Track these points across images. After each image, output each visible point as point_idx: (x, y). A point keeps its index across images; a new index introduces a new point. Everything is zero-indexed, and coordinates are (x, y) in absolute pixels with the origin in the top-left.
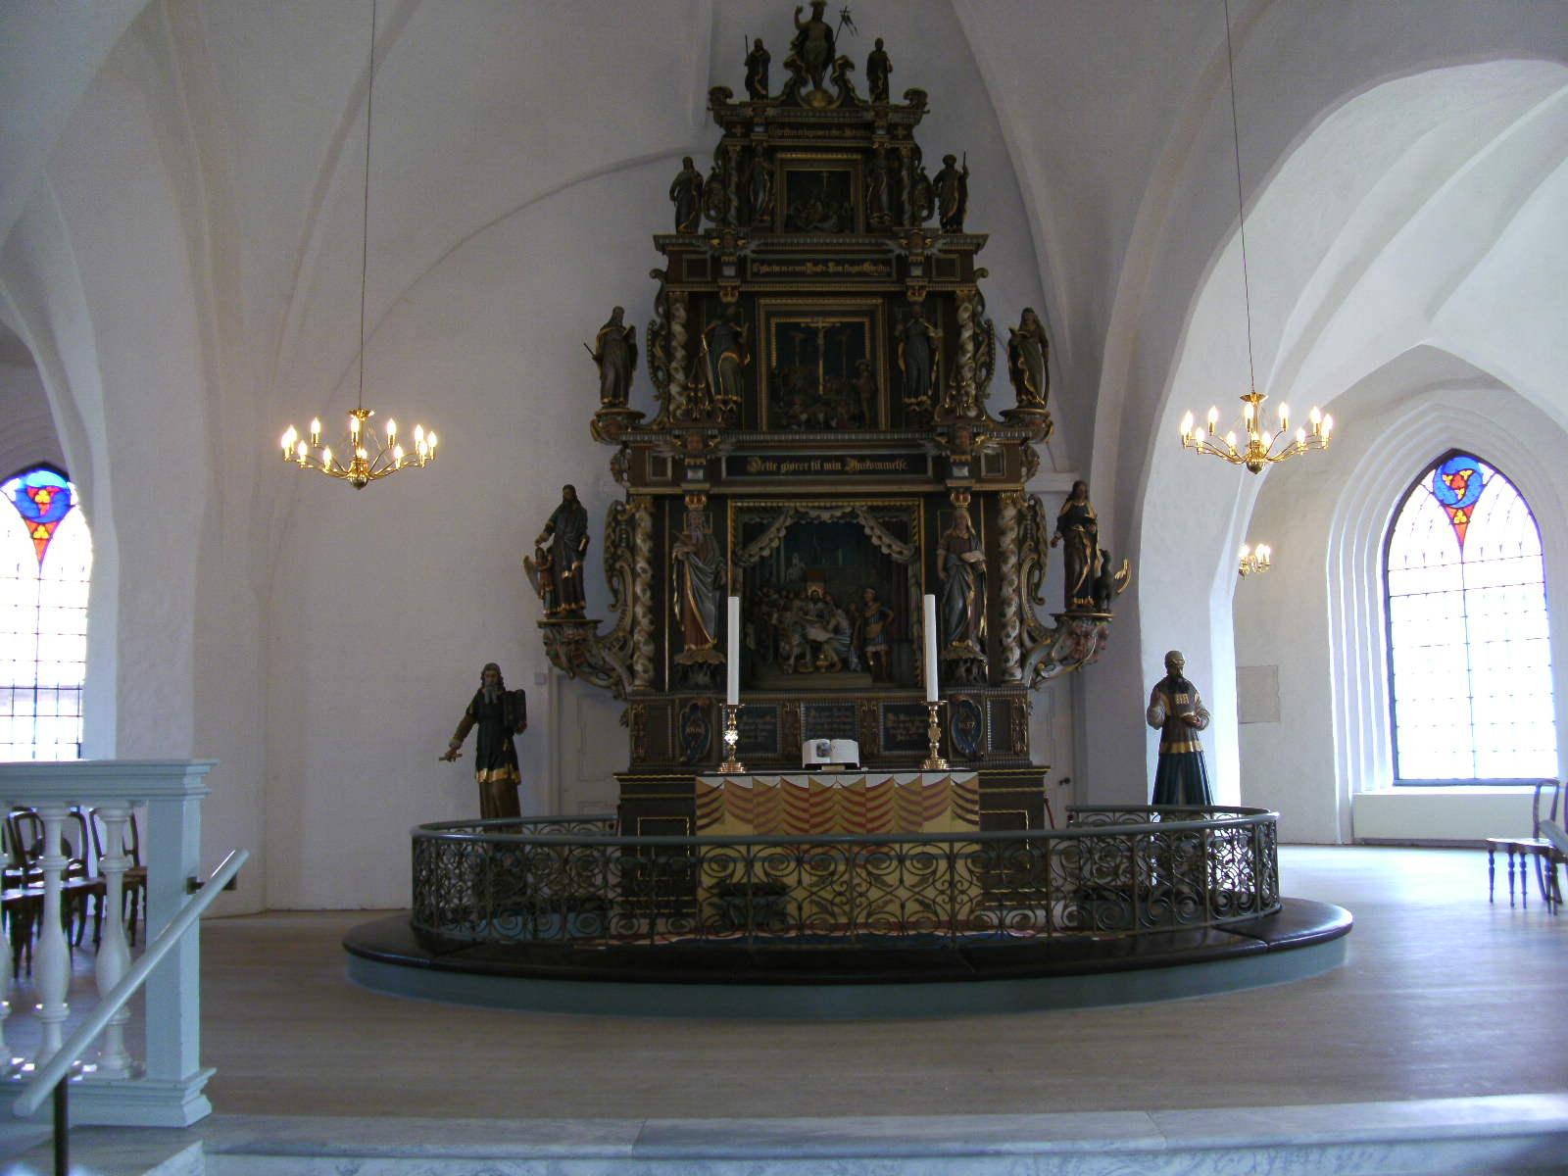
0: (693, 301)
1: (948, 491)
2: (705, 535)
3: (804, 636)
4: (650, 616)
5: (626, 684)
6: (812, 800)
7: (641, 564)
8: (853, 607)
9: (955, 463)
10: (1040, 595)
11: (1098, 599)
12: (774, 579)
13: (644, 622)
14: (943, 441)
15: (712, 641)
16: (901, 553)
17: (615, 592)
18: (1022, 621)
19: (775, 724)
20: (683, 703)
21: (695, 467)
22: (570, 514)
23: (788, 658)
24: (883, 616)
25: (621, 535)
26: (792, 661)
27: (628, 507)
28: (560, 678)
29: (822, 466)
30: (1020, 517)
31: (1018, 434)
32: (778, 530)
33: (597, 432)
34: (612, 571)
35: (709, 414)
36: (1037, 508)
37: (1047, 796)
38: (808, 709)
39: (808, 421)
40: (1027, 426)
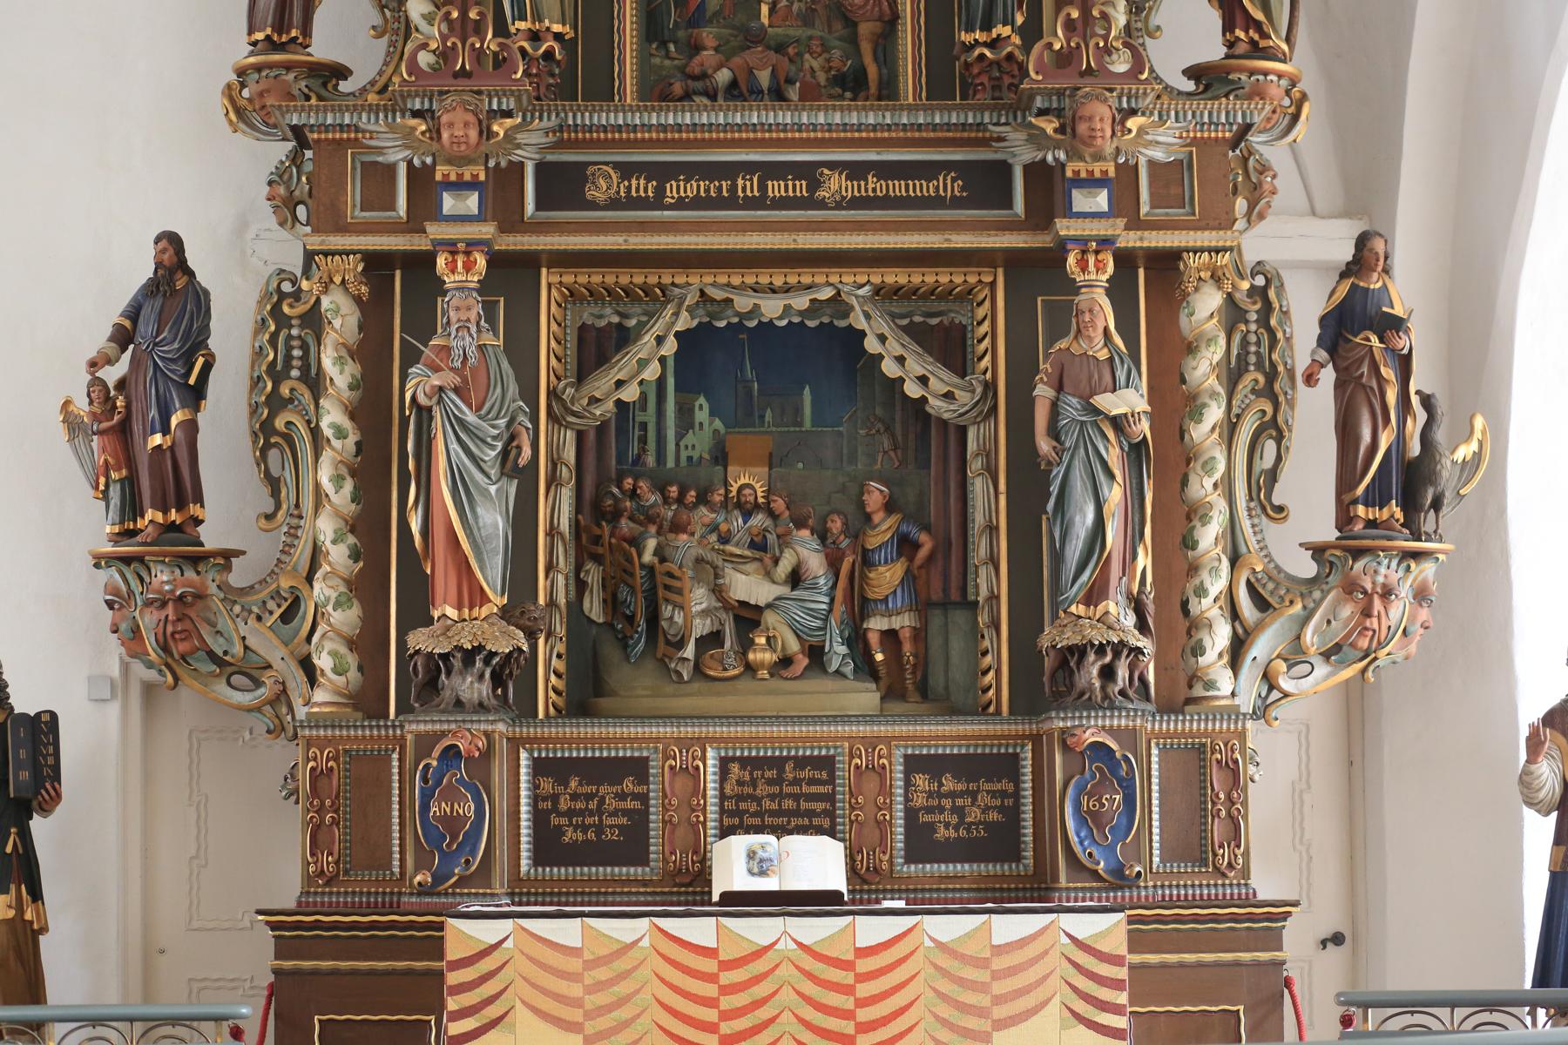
1: (1062, 247)
2: (481, 348)
3: (718, 591)
4: (351, 539)
5: (298, 703)
6: (727, 978)
7: (332, 416)
8: (836, 525)
9: (1078, 182)
10: (1276, 502)
11: (1411, 505)
12: (651, 460)
13: (338, 555)
14: (1049, 126)
15: (498, 600)
16: (949, 396)
17: (274, 484)
18: (1235, 560)
19: (644, 798)
20: (425, 743)
21: (460, 186)
22: (172, 294)
23: (681, 644)
24: (906, 545)
25: (289, 348)
26: (689, 651)
27: (305, 285)
28: (149, 689)
29: (763, 188)
30: (1233, 313)
31: (1224, 112)
32: (660, 340)
33: (239, 112)
34: (266, 436)
35: (500, 62)
36: (1272, 294)
37: (1291, 971)
38: (724, 763)
39: (734, 84)
40: (1249, 97)
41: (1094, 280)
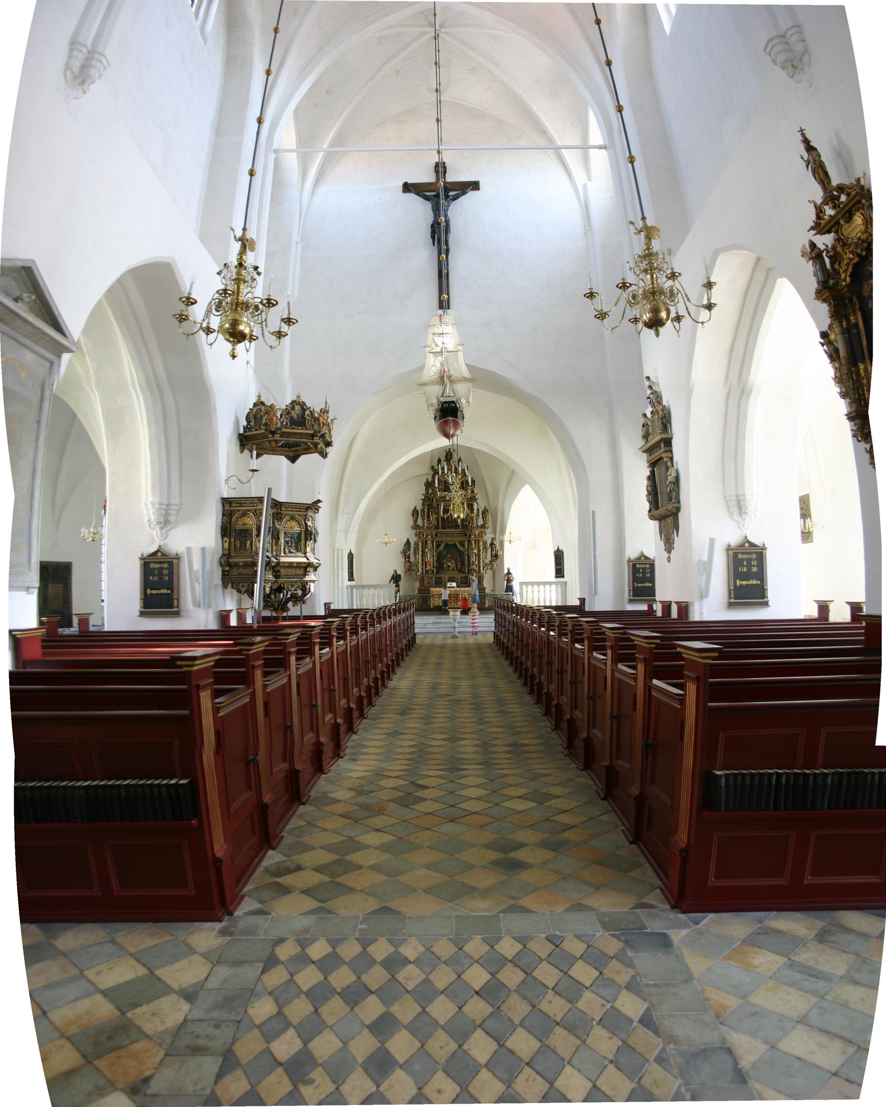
0: (428, 505)
22: (408, 542)
34: (415, 553)
41: (473, 542)
